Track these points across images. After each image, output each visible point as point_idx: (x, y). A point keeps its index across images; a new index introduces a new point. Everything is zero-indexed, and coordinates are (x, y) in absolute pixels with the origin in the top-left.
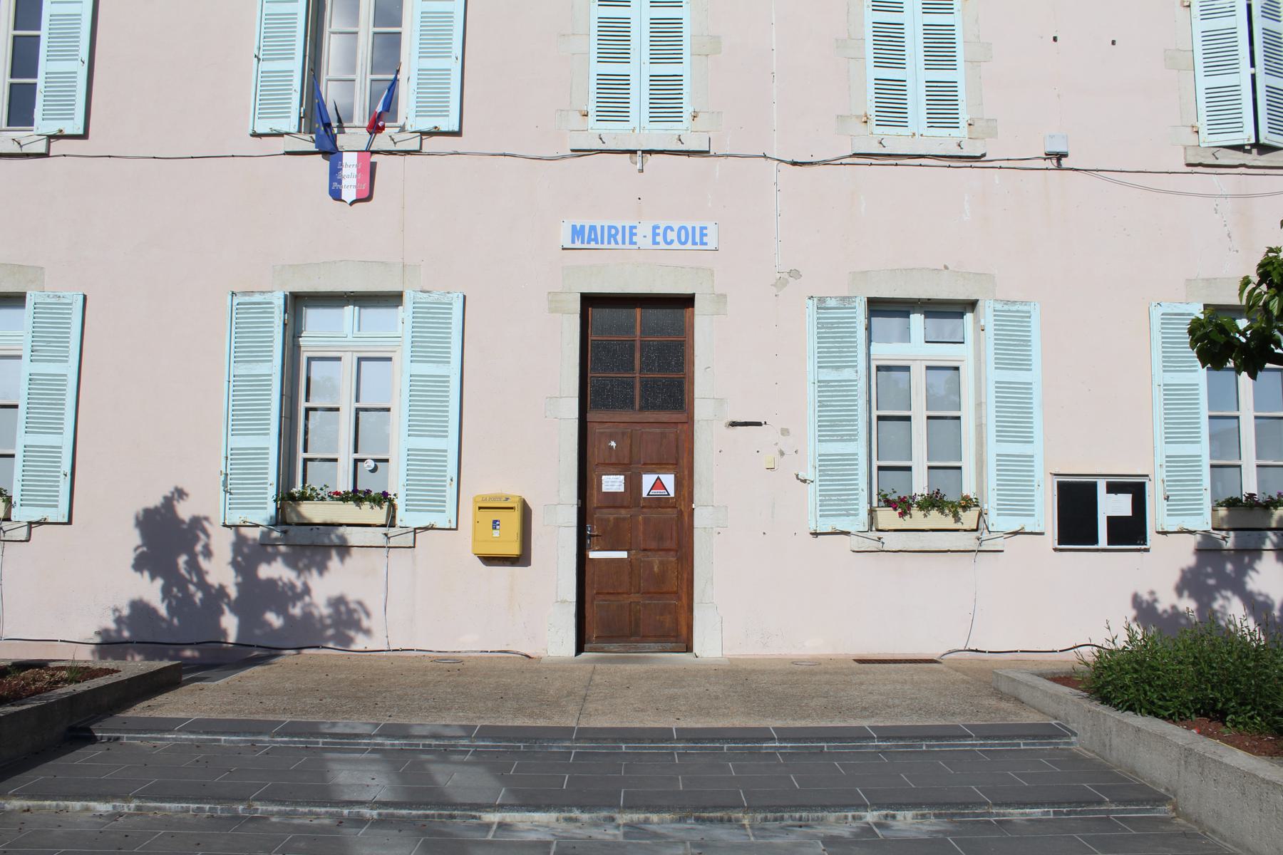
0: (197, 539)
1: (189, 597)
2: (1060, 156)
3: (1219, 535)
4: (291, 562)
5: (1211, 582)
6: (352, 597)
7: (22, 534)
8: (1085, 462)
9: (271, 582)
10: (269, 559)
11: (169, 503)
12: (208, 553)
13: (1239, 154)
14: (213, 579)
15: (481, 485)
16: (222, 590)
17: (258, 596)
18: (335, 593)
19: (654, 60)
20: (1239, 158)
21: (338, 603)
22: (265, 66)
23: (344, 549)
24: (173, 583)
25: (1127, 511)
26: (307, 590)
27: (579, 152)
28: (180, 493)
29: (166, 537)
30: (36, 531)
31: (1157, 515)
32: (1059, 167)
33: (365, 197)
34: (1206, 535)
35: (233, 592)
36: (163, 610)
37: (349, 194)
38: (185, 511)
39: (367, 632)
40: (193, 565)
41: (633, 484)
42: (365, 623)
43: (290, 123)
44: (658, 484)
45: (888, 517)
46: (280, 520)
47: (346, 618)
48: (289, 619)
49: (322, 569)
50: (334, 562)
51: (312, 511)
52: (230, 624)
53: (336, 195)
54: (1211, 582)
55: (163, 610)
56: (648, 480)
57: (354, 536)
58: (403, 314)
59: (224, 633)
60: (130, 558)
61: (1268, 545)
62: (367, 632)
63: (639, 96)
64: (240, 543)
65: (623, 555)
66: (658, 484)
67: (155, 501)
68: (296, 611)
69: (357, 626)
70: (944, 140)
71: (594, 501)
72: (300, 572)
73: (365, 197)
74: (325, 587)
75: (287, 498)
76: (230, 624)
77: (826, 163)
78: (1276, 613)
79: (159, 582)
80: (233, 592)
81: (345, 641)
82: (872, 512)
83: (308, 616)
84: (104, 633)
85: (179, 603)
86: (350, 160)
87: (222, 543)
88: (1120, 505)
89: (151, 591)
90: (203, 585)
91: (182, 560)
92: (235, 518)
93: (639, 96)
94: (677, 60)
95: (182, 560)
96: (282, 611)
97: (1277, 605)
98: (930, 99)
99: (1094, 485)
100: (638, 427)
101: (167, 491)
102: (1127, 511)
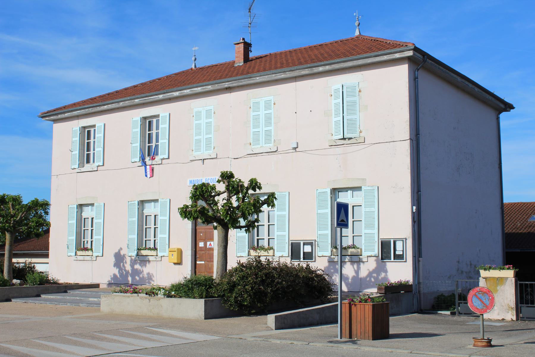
0: (124, 259)
1: (123, 273)
2: (295, 149)
3: (332, 257)
4: (140, 265)
5: (332, 271)
6: (151, 273)
7: (95, 259)
8: (296, 237)
9: (137, 269)
10: (136, 264)
11: (119, 251)
12: (126, 263)
13: (343, 141)
14: (127, 269)
15: (175, 245)
16: (128, 272)
17: (135, 272)
18: (148, 272)
19: (207, 134)
20: (343, 142)
21: (148, 274)
22: (133, 145)
23: (149, 261)
24: (120, 269)
25: (310, 251)
26: (143, 271)
27: (192, 161)
28: (121, 249)
29: (119, 258)
30: (98, 258)
31: (318, 252)
32: (296, 151)
33: (152, 176)
34: (329, 257)
35: (130, 272)
36: (119, 276)
37: (149, 176)
38: (122, 253)
39: (153, 281)
40: (124, 265)
41: (205, 244)
42: (153, 279)
43: (137, 159)
44: (210, 245)
45: (252, 251)
46: (137, 255)
47: (150, 277)
48: (140, 278)
49: (145, 266)
50: (147, 265)
51: (144, 252)
52: (130, 279)
53: (146, 176)
54: (332, 271)
55: (119, 276)
56: (208, 243)
57: (151, 258)
58: (159, 204)
59: (129, 281)
60: (113, 264)
61: (347, 260)
62: (153, 281)
63: (203, 144)
64: (131, 260)
65: (203, 262)
66: (210, 245)
67: (117, 251)
68: (141, 276)
69: (151, 279)
70: (271, 146)
71: (198, 249)
72: (142, 266)
73: (152, 176)
74: (147, 270)
75: (139, 249)
76: (130, 279)
77: (241, 158)
78: (350, 280)
79: (118, 269)
80: (130, 272)
81: (150, 283)
82: (249, 252)
83: (143, 277)
84: (109, 281)
85: (121, 274)
86: (148, 167)
87: (128, 260)
88: (308, 249)
89: (116, 271)
90: (125, 270)
91: (122, 264)
92: (130, 255)
93: (203, 144)
94: (210, 133)
95: (122, 264)
96: (139, 276)
97: (350, 278)
98: (266, 135)
99: (300, 243)
100: (208, 230)
101: (119, 248)
102: (310, 251)
